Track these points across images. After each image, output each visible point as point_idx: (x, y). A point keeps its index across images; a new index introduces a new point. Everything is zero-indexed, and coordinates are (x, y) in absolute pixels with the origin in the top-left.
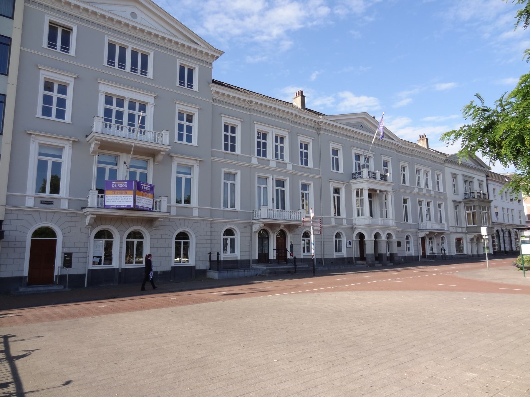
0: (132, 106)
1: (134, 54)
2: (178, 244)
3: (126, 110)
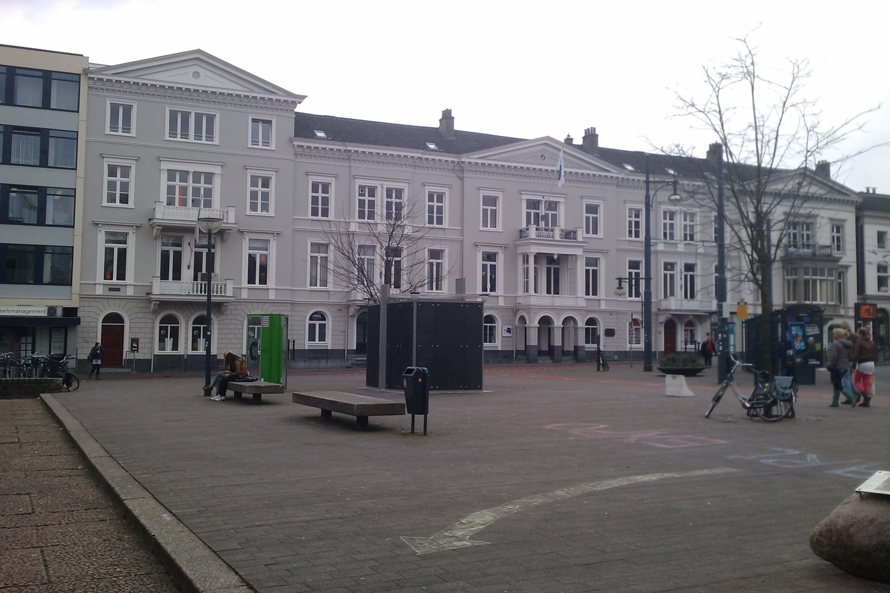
0: (197, 180)
1: (199, 117)
2: (312, 327)
3: (190, 184)
